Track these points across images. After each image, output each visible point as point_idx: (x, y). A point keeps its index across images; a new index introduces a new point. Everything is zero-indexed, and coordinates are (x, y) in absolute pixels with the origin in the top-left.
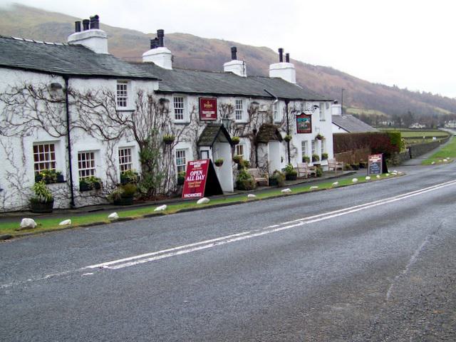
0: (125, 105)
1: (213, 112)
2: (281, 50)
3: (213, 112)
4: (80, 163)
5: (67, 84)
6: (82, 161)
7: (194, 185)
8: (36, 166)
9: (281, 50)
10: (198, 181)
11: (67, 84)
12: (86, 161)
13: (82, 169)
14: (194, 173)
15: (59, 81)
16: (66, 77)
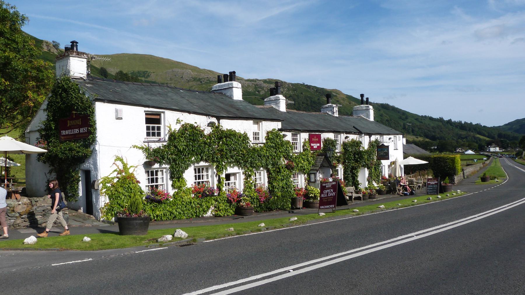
0: (258, 139)
1: (318, 145)
2: (362, 96)
3: (318, 145)
4: (196, 176)
5: (219, 123)
6: (197, 174)
7: (328, 199)
8: (298, 183)
9: (362, 96)
10: (330, 196)
11: (219, 123)
12: (201, 174)
13: (198, 181)
14: (326, 191)
15: (214, 120)
16: (219, 118)
